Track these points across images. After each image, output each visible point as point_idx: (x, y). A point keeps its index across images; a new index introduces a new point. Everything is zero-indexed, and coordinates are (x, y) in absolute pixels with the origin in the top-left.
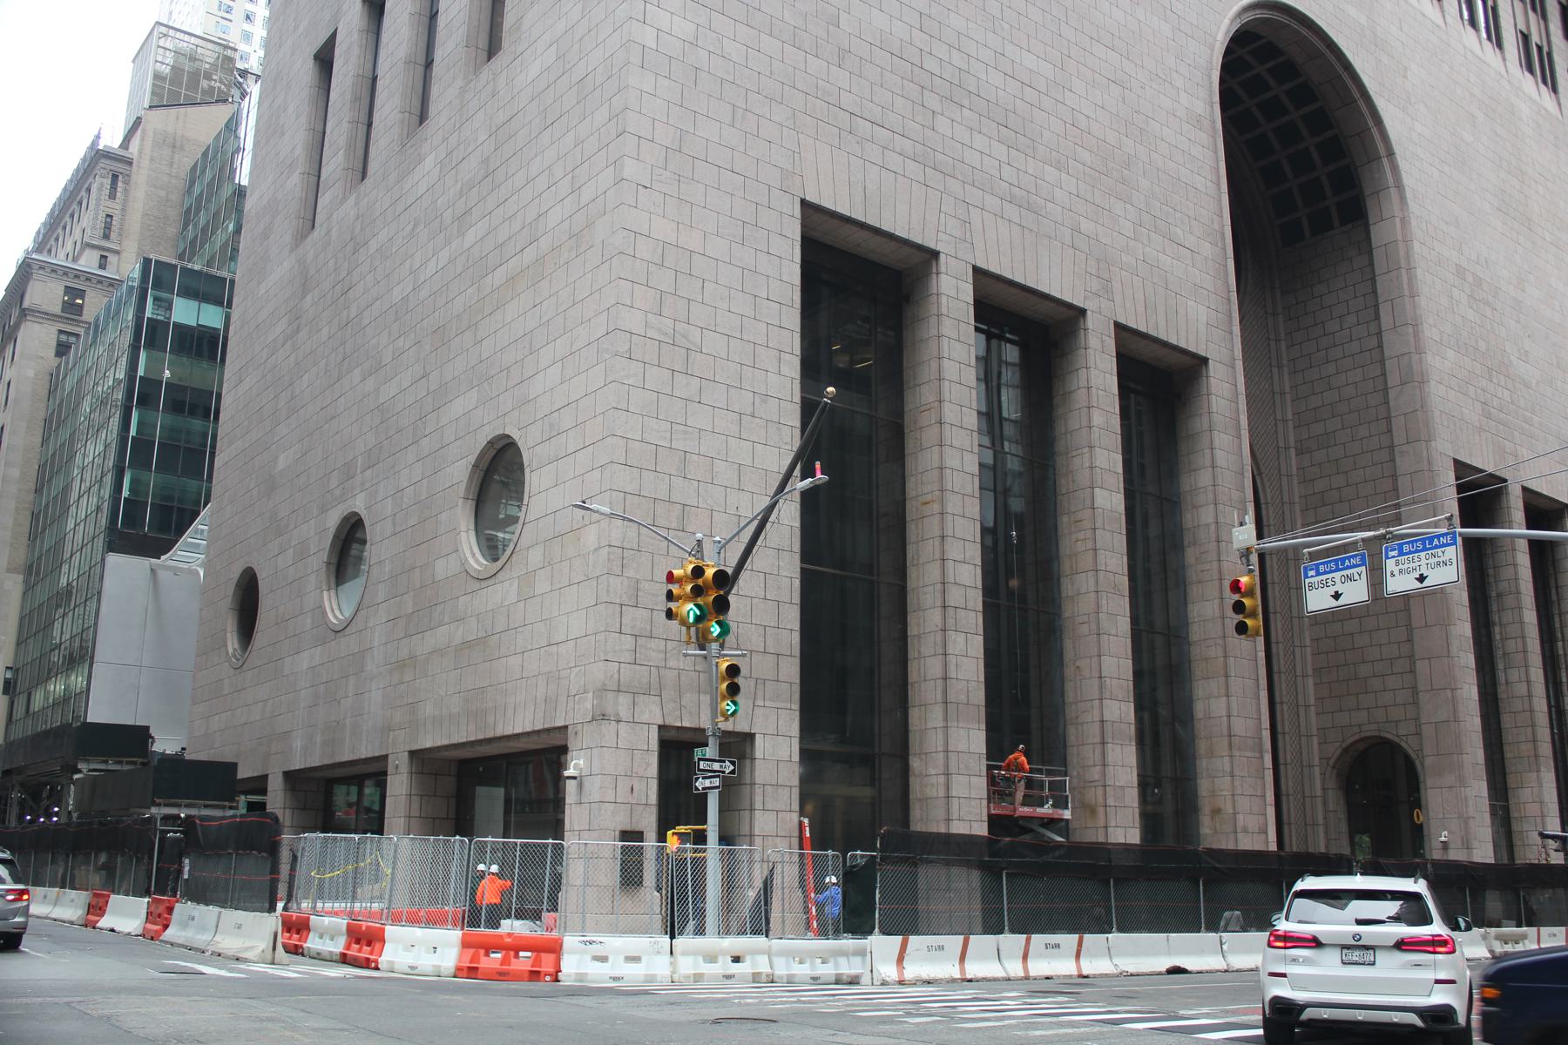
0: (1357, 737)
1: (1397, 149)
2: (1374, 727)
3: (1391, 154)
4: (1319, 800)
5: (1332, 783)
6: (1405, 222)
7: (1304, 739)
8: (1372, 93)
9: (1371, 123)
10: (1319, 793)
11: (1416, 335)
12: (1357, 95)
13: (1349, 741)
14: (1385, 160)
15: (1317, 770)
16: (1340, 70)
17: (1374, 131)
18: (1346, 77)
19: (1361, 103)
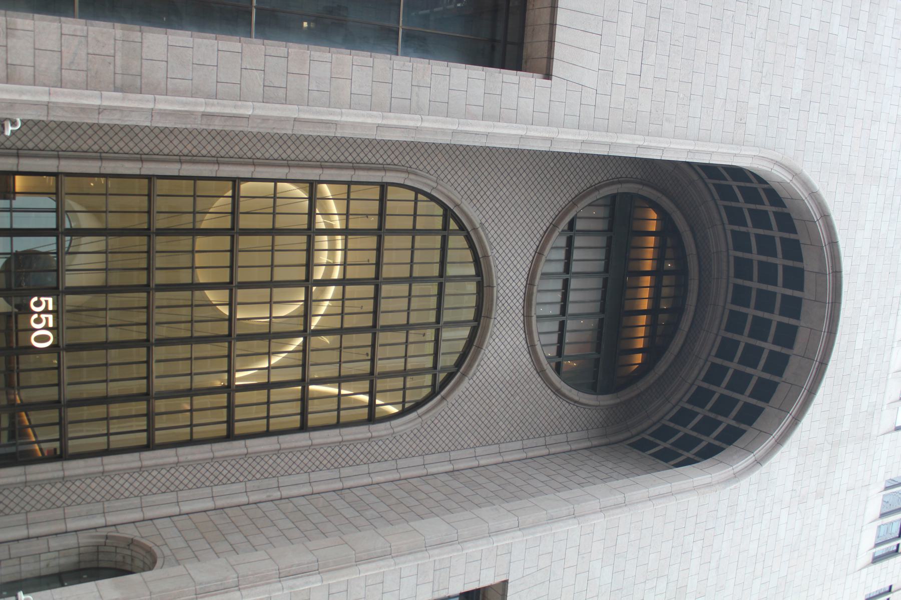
0: (151, 545)
1: (766, 465)
2: (167, 552)
3: (759, 462)
4: (60, 527)
5: (85, 539)
6: (709, 485)
7: (137, 501)
8: (800, 425)
9: (777, 434)
10: (72, 525)
11: (617, 506)
12: (794, 410)
13: (143, 541)
14: (750, 459)
15: (100, 521)
16: (807, 385)
17: (770, 441)
18: (803, 393)
19: (788, 419)
